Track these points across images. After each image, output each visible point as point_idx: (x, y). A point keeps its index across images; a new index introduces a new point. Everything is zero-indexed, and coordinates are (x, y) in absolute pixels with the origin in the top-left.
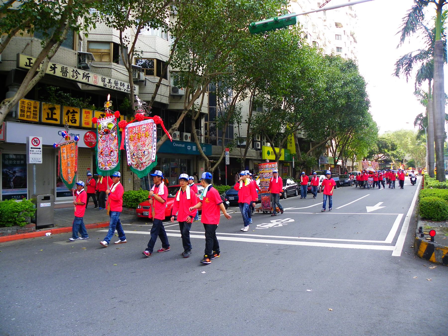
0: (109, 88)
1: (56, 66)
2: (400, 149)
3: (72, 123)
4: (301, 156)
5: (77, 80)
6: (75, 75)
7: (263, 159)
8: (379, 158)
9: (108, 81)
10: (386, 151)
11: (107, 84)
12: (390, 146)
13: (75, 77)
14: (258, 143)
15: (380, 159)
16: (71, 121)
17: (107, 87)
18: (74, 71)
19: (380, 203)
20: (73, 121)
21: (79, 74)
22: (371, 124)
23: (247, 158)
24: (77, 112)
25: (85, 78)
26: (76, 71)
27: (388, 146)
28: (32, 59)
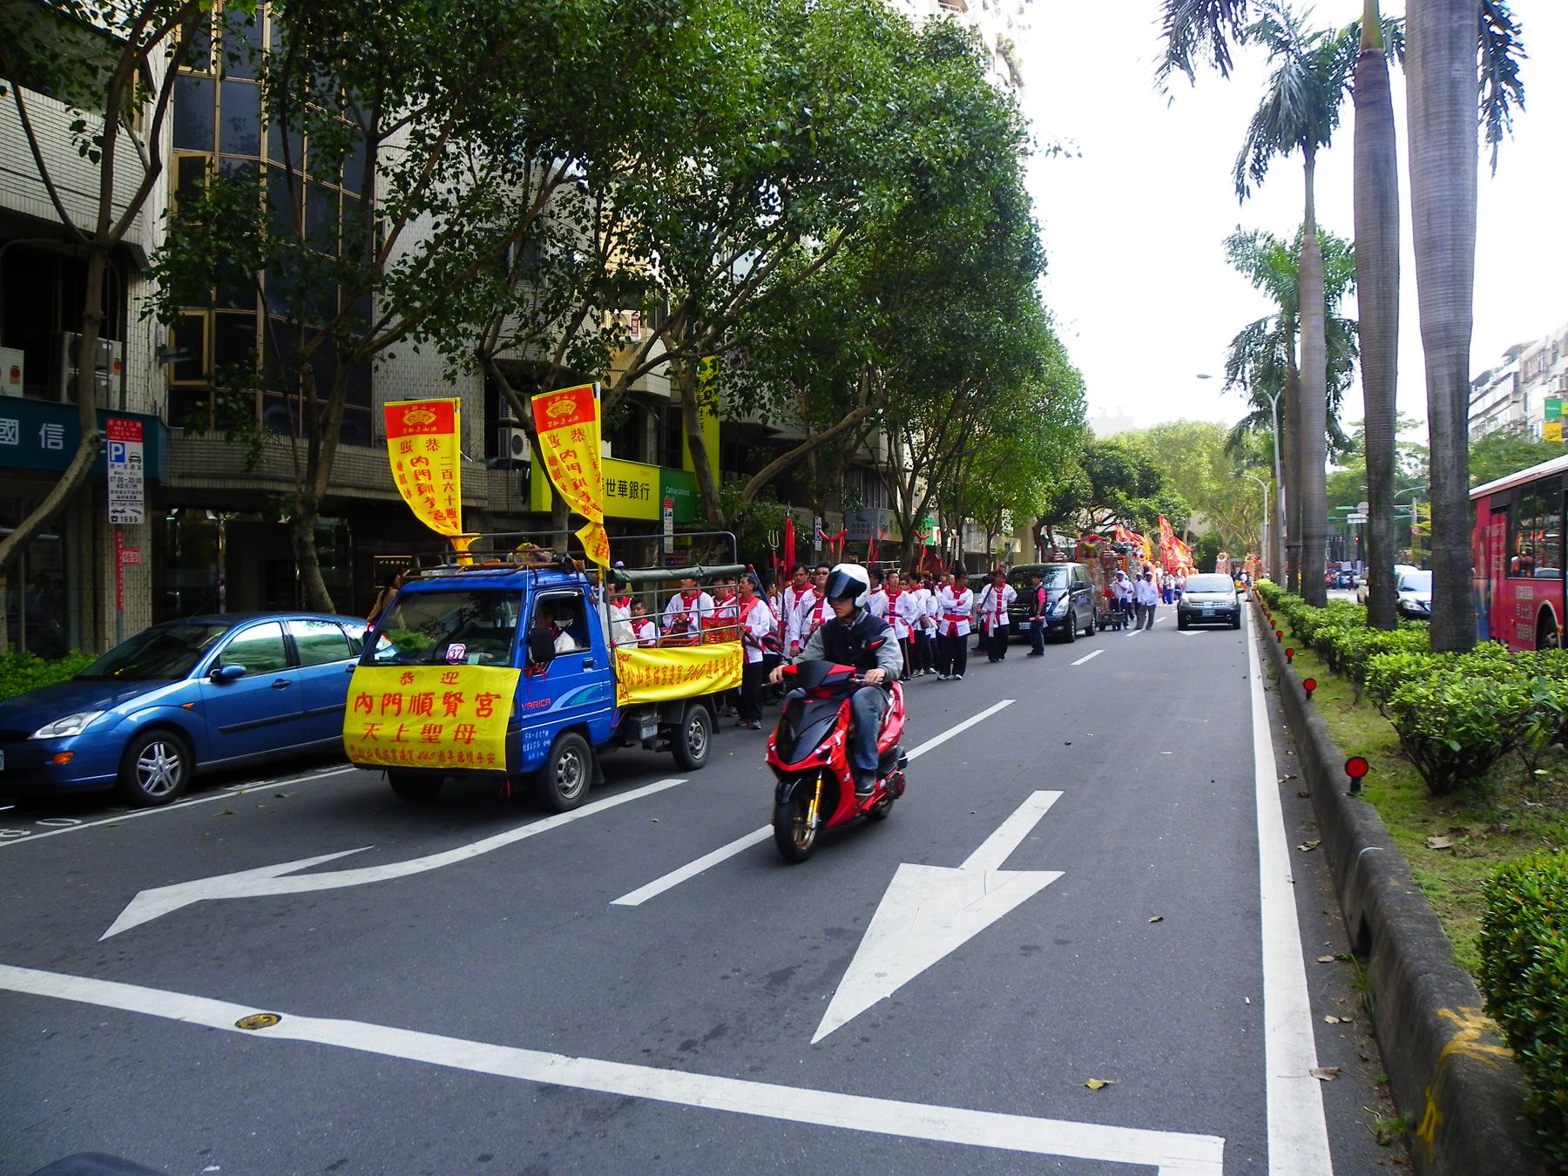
2: (1172, 493)
4: (716, 497)
7: (534, 509)
8: (1094, 526)
10: (1121, 495)
12: (1136, 476)
14: (515, 432)
15: (1099, 529)
19: (1041, 802)
22: (1050, 368)
23: (330, 492)
27: (1130, 476)
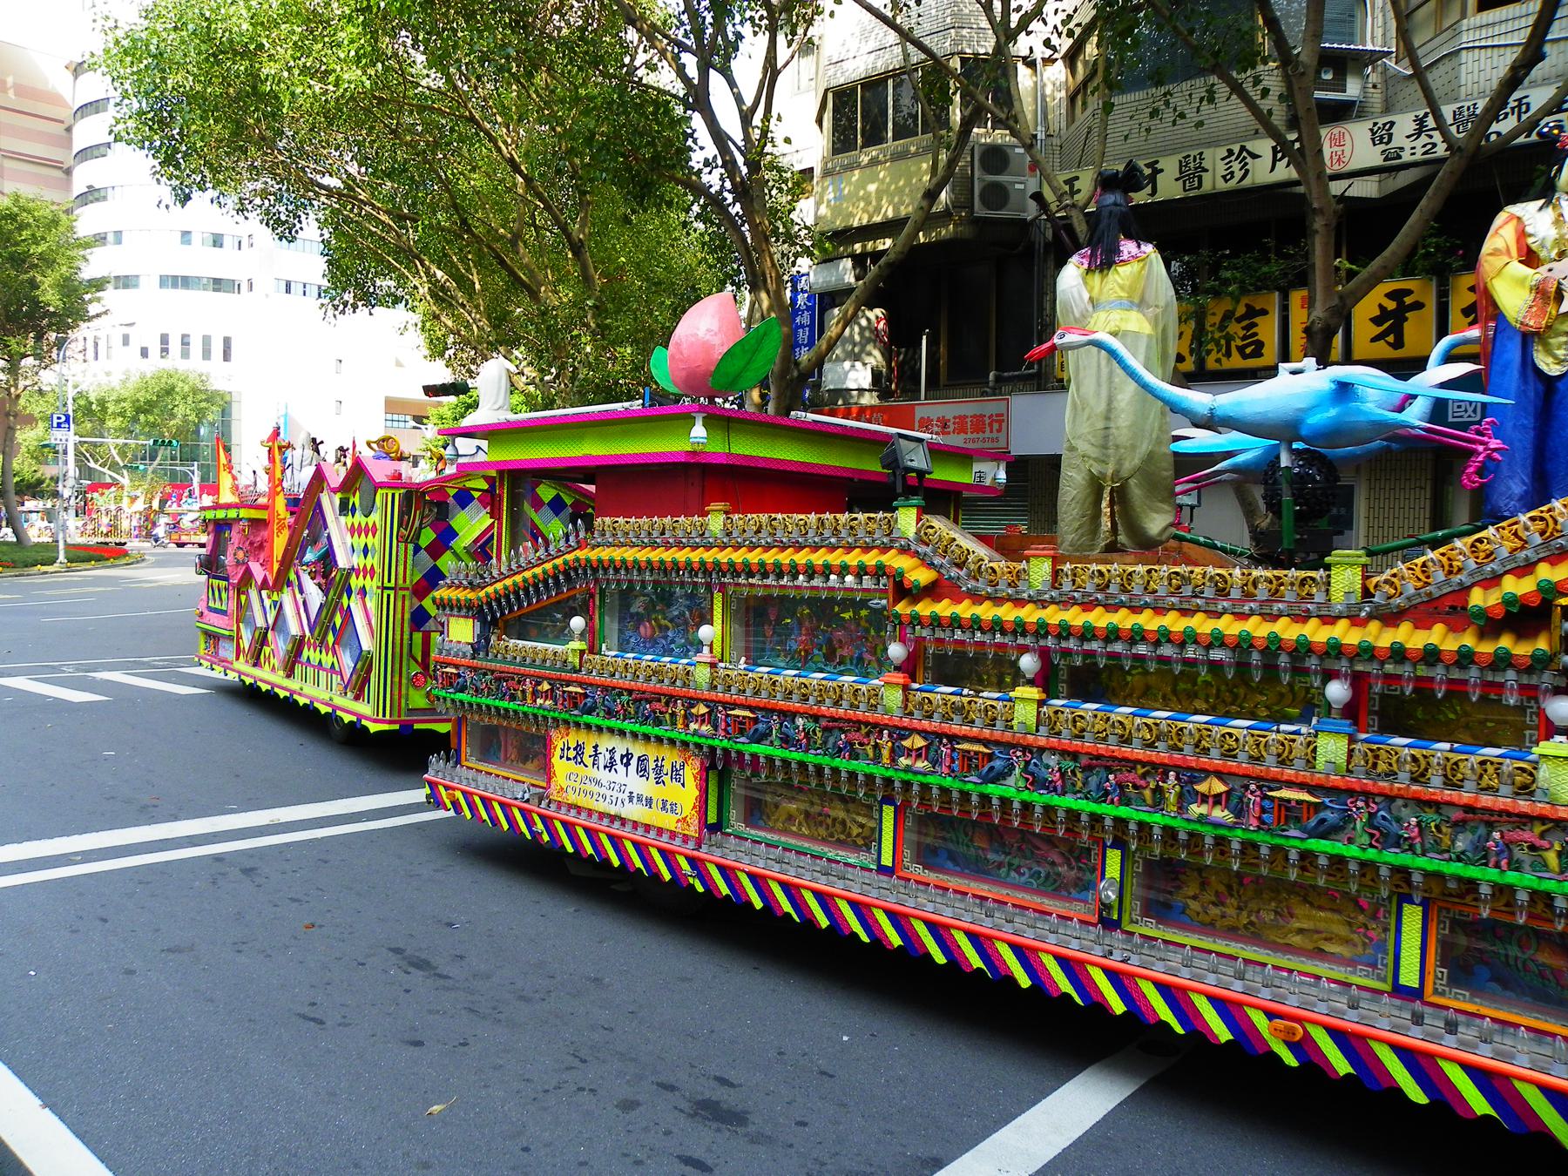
0: (1418, 157)
1: (1159, 166)
3: (1245, 356)
5: (1247, 182)
6: (1236, 166)
9: (1411, 127)
11: (1407, 144)
13: (1238, 175)
16: (1241, 350)
17: (1406, 157)
18: (1231, 152)
20: (1248, 351)
21: (1255, 156)
24: (1264, 312)
25: (1281, 165)
26: (1243, 148)
28: (1077, 178)
